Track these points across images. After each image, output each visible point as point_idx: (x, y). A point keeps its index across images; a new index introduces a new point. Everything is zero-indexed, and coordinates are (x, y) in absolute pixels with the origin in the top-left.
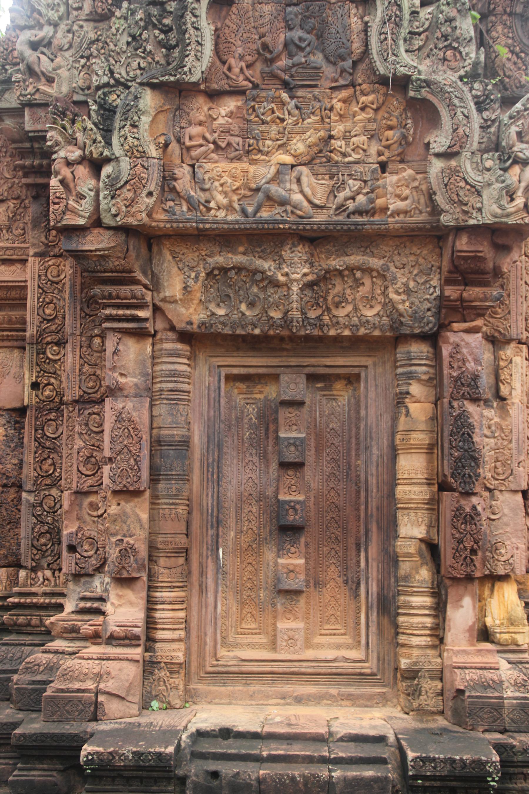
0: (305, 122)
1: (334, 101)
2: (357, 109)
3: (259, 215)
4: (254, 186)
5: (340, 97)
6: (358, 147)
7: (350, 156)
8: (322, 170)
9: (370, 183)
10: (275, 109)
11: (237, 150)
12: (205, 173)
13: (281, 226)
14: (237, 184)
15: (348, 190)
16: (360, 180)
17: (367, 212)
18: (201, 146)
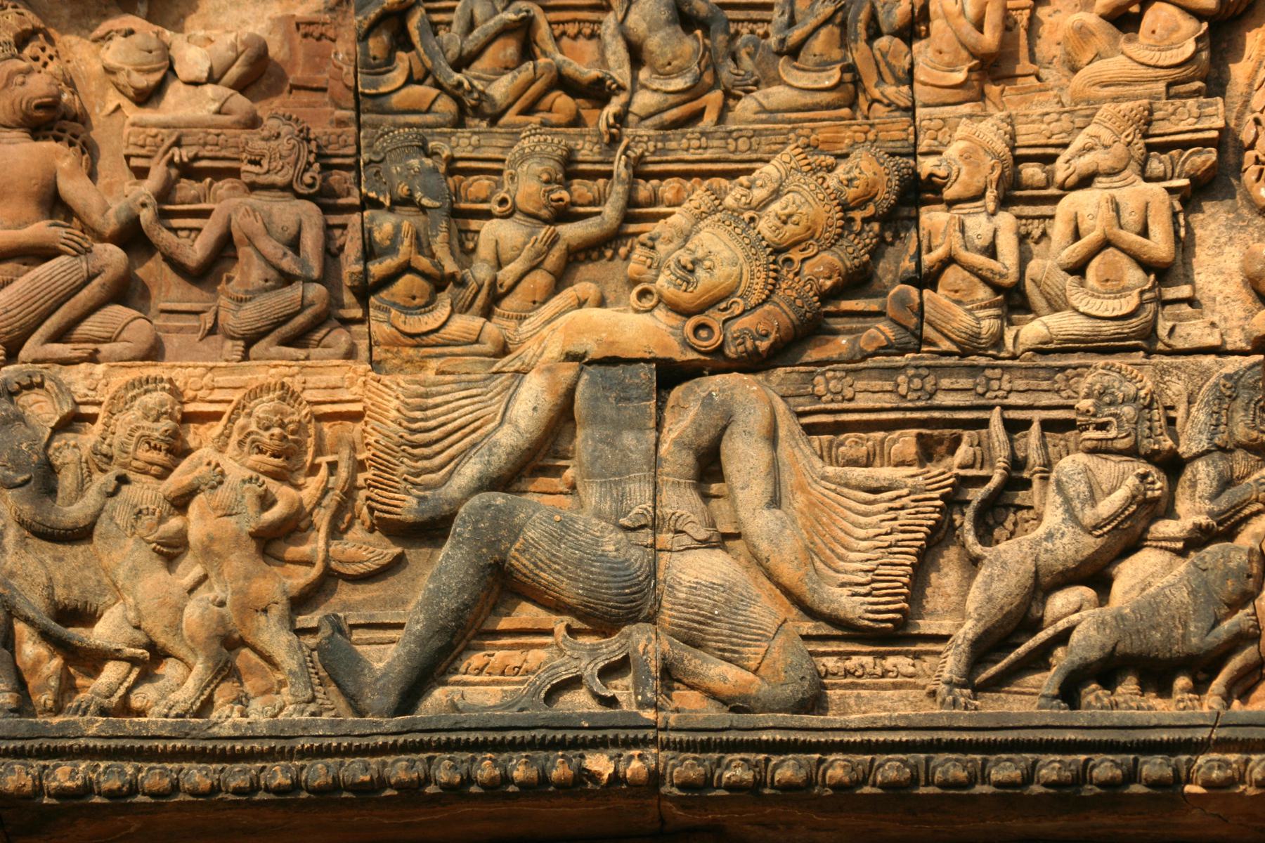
0: (745, 107)
3: (439, 695)
4: (407, 506)
7: (1055, 306)
8: (870, 396)
9: (1203, 473)
10: (543, 32)
11: (287, 279)
12: (72, 421)
13: (600, 764)
14: (285, 497)
15: (1053, 516)
16: (1132, 452)
17: (1202, 667)
18: (39, 254)
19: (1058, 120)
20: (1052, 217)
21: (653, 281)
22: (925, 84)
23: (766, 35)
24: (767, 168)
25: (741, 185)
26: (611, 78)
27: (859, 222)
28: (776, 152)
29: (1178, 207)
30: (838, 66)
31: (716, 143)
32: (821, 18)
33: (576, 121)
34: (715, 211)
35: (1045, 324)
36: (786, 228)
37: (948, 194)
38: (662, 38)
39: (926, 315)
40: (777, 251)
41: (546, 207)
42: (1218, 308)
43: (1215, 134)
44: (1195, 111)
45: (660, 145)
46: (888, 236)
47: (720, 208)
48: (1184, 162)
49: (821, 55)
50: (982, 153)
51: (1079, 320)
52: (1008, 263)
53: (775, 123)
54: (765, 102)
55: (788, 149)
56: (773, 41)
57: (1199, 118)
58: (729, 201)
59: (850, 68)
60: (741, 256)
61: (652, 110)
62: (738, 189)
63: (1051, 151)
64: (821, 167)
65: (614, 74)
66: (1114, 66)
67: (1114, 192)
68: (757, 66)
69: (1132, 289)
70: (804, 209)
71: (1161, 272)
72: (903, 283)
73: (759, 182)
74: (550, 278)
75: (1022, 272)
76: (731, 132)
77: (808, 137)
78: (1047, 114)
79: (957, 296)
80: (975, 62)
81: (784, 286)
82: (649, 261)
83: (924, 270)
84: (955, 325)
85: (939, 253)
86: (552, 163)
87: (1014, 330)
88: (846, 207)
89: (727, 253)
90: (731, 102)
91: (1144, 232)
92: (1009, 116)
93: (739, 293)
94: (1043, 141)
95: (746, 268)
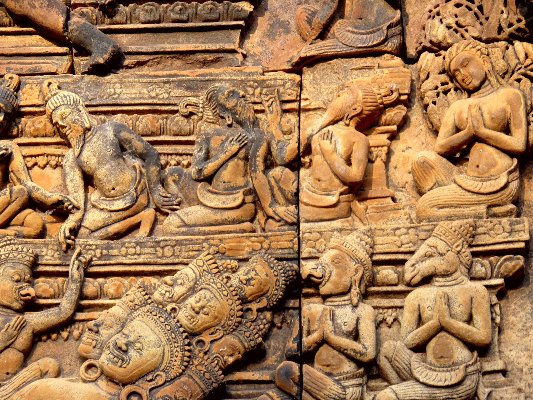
0: (171, 222)
1: (313, 124)
2: (432, 156)
5: (343, 101)
6: (442, 329)
19: (405, 234)
20: (401, 307)
21: (97, 358)
22: (307, 205)
23: (189, 165)
24: (186, 270)
25: (166, 283)
26: (69, 200)
27: (255, 312)
28: (193, 257)
29: (495, 299)
30: (242, 190)
31: (147, 250)
32: (229, 154)
33: (42, 234)
34: (145, 304)
35: (394, 391)
36: (198, 317)
37: (324, 289)
38: (108, 170)
39: (304, 384)
40: (192, 334)
41: (17, 300)
42: (524, 377)
43: (522, 245)
44: (508, 228)
45: (105, 252)
46: (277, 320)
47: (149, 301)
48: (500, 266)
49: (229, 182)
50: (348, 259)
51: (419, 388)
52: (366, 344)
53: (193, 234)
54: (185, 219)
55: (201, 256)
56: (193, 170)
57: (511, 232)
58: (157, 296)
59: (252, 192)
60: (164, 339)
61: (99, 225)
62: (164, 286)
63: (401, 257)
64: (227, 269)
65: (70, 197)
66: (447, 192)
67: (446, 289)
68: (181, 190)
69: (460, 365)
70: (212, 303)
71: (482, 350)
72: (289, 358)
73: (179, 281)
74: (21, 355)
75: (378, 352)
76: (159, 242)
77: (217, 246)
78: (398, 229)
79: (328, 370)
80: (346, 188)
81: (196, 362)
82: (94, 342)
83: (304, 349)
84: (326, 392)
85: (315, 336)
86: (22, 267)
87: (373, 393)
88: (244, 301)
89: (153, 337)
90: (161, 217)
91: (470, 320)
92: (370, 230)
93: (162, 368)
94: (395, 249)
95: (167, 348)
